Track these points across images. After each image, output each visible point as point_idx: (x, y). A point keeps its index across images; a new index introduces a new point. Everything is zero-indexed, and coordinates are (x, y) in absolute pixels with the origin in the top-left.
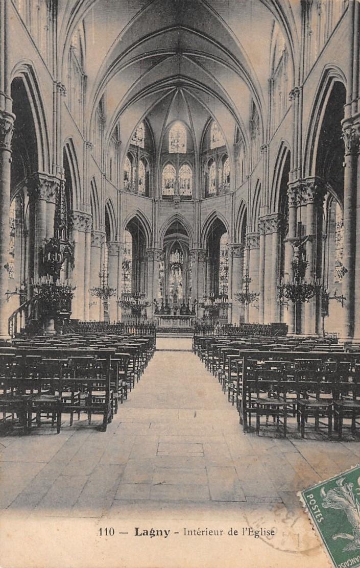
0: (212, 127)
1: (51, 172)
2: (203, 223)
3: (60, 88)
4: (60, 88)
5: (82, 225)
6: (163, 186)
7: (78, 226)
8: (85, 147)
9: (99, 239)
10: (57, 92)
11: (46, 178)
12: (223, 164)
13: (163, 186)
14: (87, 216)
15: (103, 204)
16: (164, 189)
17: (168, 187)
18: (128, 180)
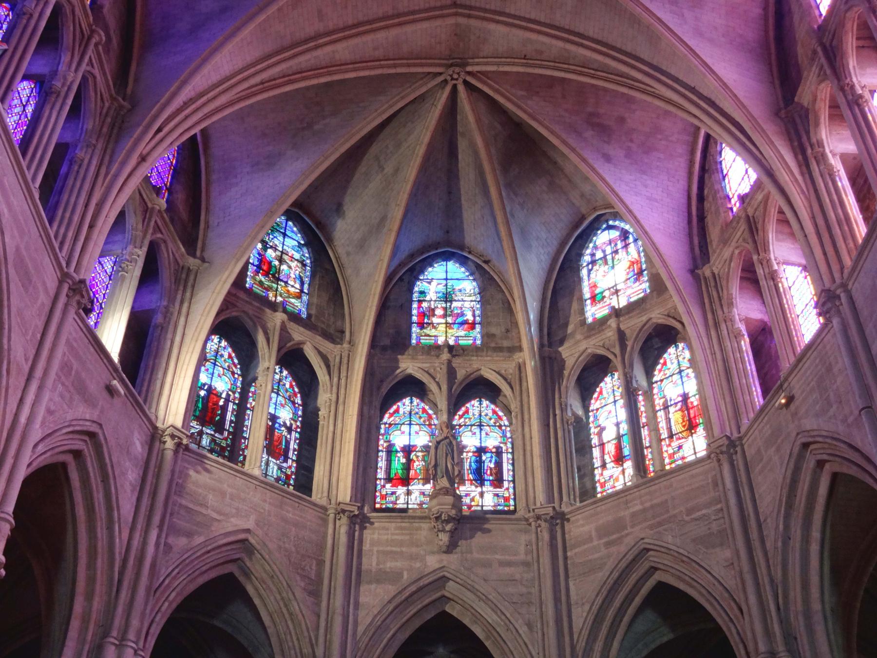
0: (587, 258)
2: (581, 617)
6: (381, 474)
12: (649, 373)
13: (381, 474)
17: (405, 481)
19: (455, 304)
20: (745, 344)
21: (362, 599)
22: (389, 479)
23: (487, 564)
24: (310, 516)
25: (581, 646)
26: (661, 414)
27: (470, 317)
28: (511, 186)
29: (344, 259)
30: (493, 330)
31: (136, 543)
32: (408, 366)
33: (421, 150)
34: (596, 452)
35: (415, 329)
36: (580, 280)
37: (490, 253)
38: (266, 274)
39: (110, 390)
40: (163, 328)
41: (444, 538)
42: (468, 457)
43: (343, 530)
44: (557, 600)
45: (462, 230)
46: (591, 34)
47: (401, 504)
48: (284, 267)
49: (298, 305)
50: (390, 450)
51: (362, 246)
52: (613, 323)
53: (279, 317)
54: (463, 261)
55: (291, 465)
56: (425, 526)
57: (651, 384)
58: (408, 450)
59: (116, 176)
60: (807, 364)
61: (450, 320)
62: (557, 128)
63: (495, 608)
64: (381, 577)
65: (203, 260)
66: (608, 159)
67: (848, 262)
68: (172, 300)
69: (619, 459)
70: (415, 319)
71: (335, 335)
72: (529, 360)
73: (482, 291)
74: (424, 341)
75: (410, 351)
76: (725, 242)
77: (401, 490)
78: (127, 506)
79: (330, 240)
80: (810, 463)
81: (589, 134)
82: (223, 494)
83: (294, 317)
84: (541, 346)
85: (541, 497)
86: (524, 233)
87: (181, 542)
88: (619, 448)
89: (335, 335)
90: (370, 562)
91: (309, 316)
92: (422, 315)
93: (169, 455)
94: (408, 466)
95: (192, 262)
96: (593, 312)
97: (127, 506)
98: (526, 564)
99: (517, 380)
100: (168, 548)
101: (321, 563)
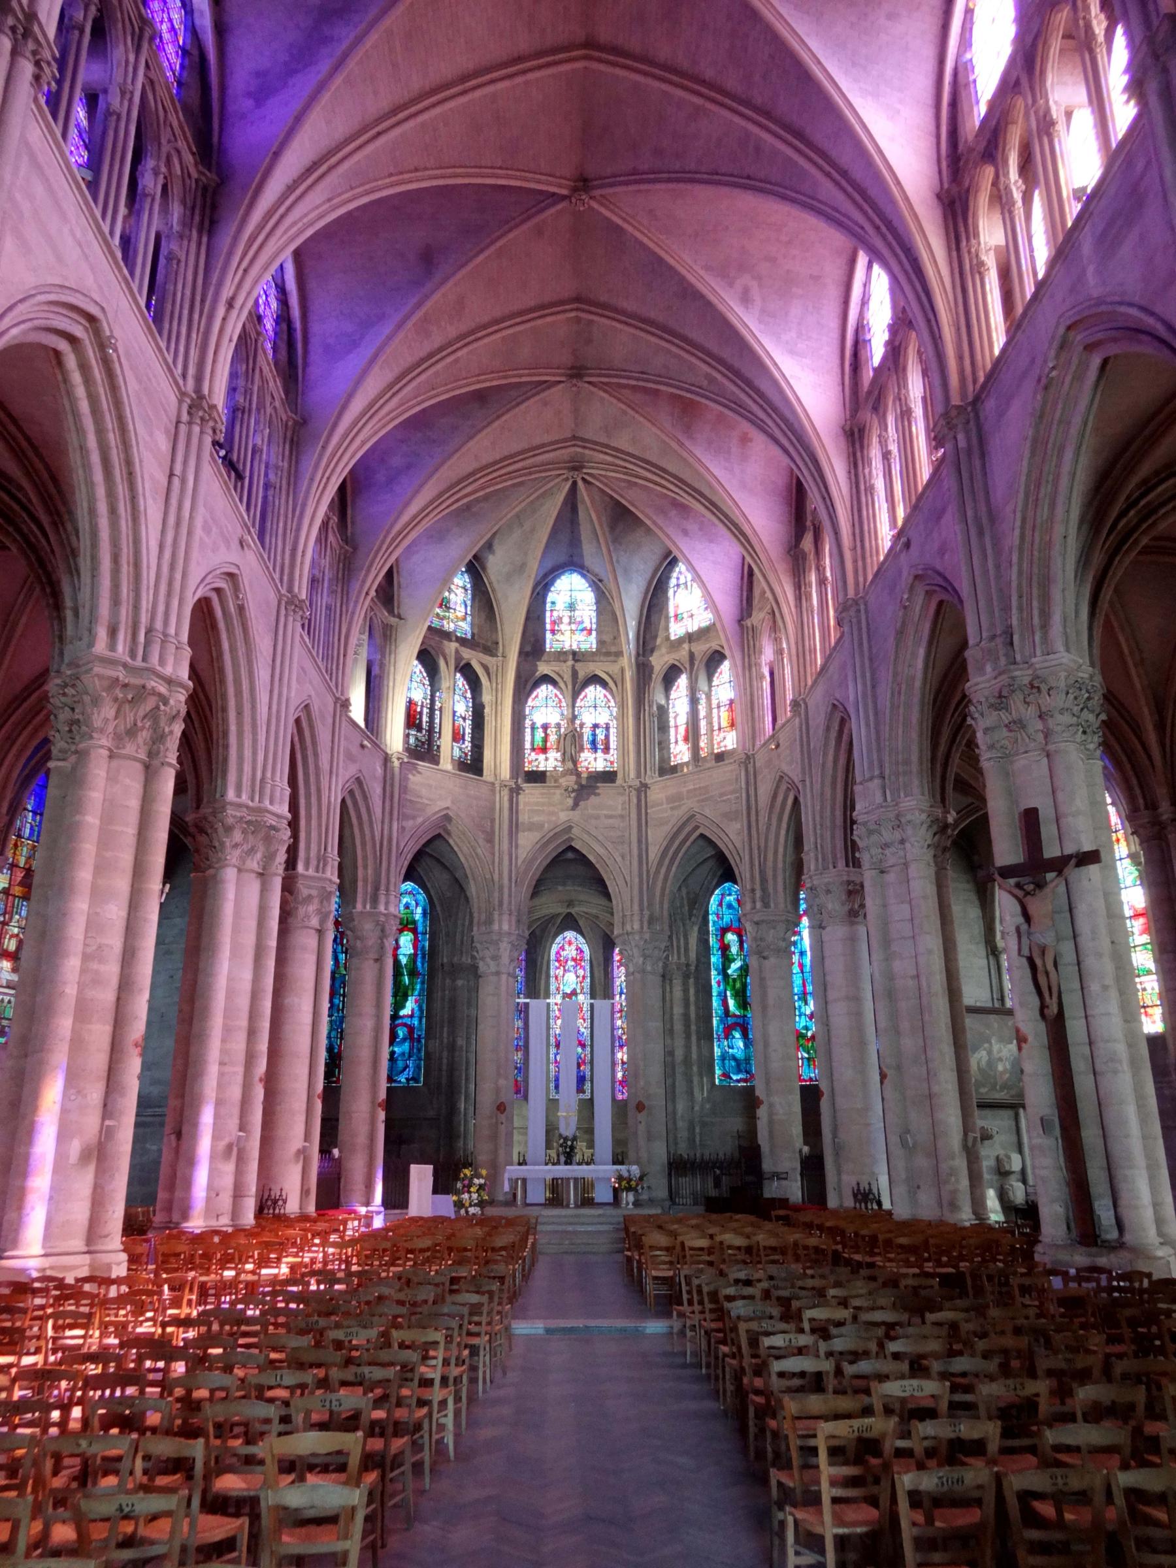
0: (673, 582)
1: (140, 657)
2: (654, 853)
3: (201, 413)
4: (201, 413)
5: (252, 851)
6: (528, 745)
7: (237, 853)
8: (283, 612)
9: (316, 901)
10: (190, 423)
11: (121, 674)
14: (272, 821)
15: (334, 794)
16: (530, 756)
17: (544, 750)
18: (419, 729)
19: (577, 613)
20: (766, 684)
21: (520, 842)
22: (533, 749)
23: (597, 817)
24: (485, 790)
25: (653, 870)
26: (715, 711)
27: (587, 624)
28: (616, 540)
29: (495, 585)
30: (607, 638)
31: (386, 832)
32: (543, 668)
33: (551, 522)
34: (672, 731)
35: (548, 635)
36: (667, 599)
37: (602, 575)
38: (441, 606)
39: (363, 746)
40: (381, 677)
41: (570, 802)
42: (587, 733)
43: (506, 798)
44: (640, 841)
45: (582, 556)
46: (670, 468)
47: (542, 768)
48: (452, 596)
49: (465, 628)
50: (533, 728)
51: (509, 577)
52: (686, 646)
53: (453, 646)
54: (583, 576)
55: (467, 745)
56: (558, 792)
57: (710, 686)
58: (545, 727)
59: (353, 613)
60: (787, 728)
61: (574, 627)
62: (647, 510)
63: (603, 845)
64: (532, 827)
65: (400, 617)
66: (685, 533)
67: (810, 683)
68: (383, 655)
69: (686, 739)
70: (548, 627)
71: (490, 648)
72: (627, 662)
73: (597, 603)
74: (557, 647)
75: (545, 657)
76: (761, 609)
77: (542, 757)
78: (378, 811)
79: (484, 569)
80: (783, 787)
81: (673, 513)
82: (430, 786)
83: (462, 641)
84: (638, 655)
85: (632, 775)
86: (626, 571)
87: (409, 824)
88: (687, 731)
89: (490, 648)
90: (524, 818)
91: (473, 635)
92: (553, 623)
93: (397, 771)
94: (545, 740)
95: (393, 620)
96: (676, 630)
97: (378, 811)
98: (622, 816)
99: (619, 681)
100: (403, 828)
101: (493, 821)
